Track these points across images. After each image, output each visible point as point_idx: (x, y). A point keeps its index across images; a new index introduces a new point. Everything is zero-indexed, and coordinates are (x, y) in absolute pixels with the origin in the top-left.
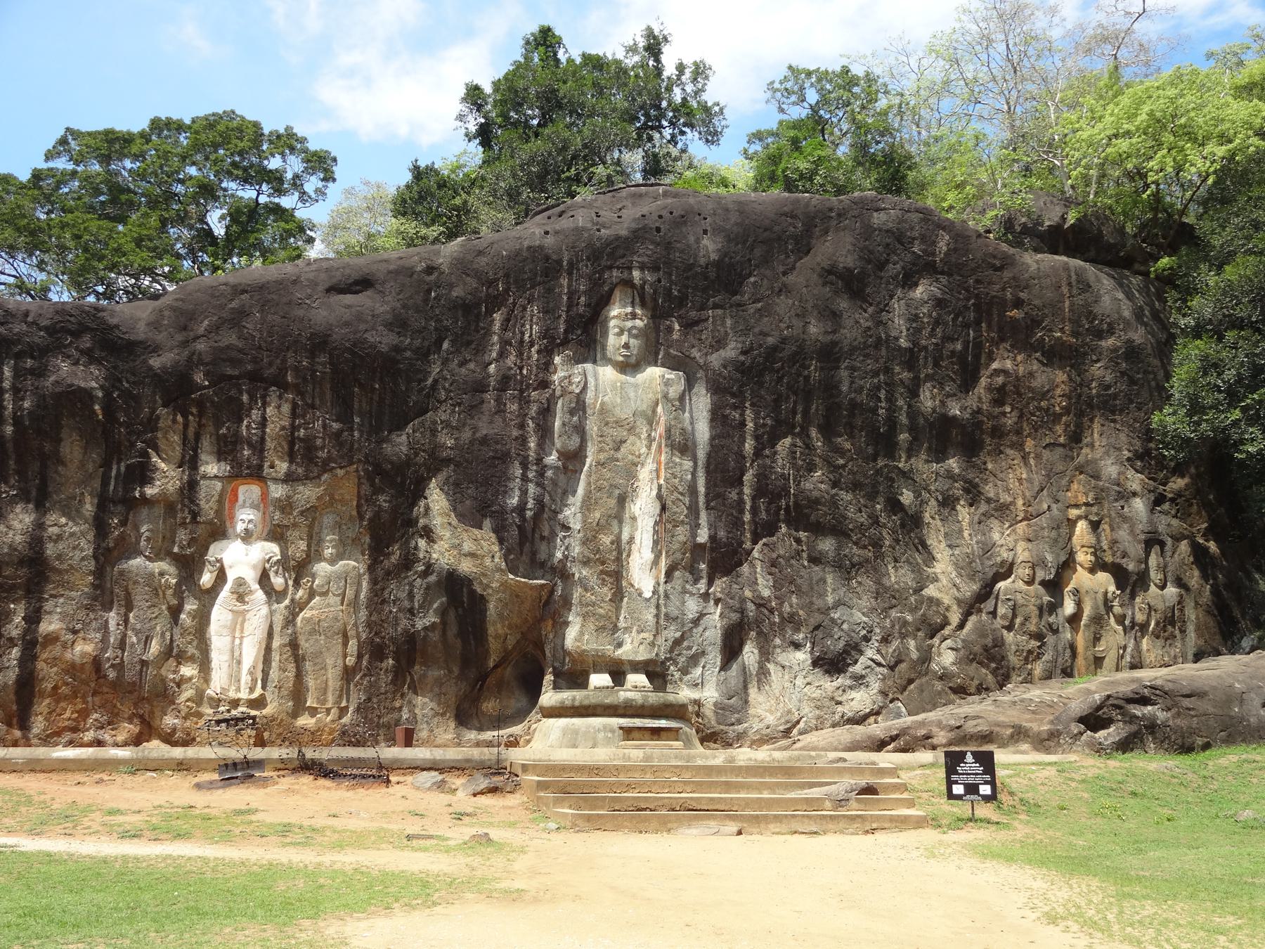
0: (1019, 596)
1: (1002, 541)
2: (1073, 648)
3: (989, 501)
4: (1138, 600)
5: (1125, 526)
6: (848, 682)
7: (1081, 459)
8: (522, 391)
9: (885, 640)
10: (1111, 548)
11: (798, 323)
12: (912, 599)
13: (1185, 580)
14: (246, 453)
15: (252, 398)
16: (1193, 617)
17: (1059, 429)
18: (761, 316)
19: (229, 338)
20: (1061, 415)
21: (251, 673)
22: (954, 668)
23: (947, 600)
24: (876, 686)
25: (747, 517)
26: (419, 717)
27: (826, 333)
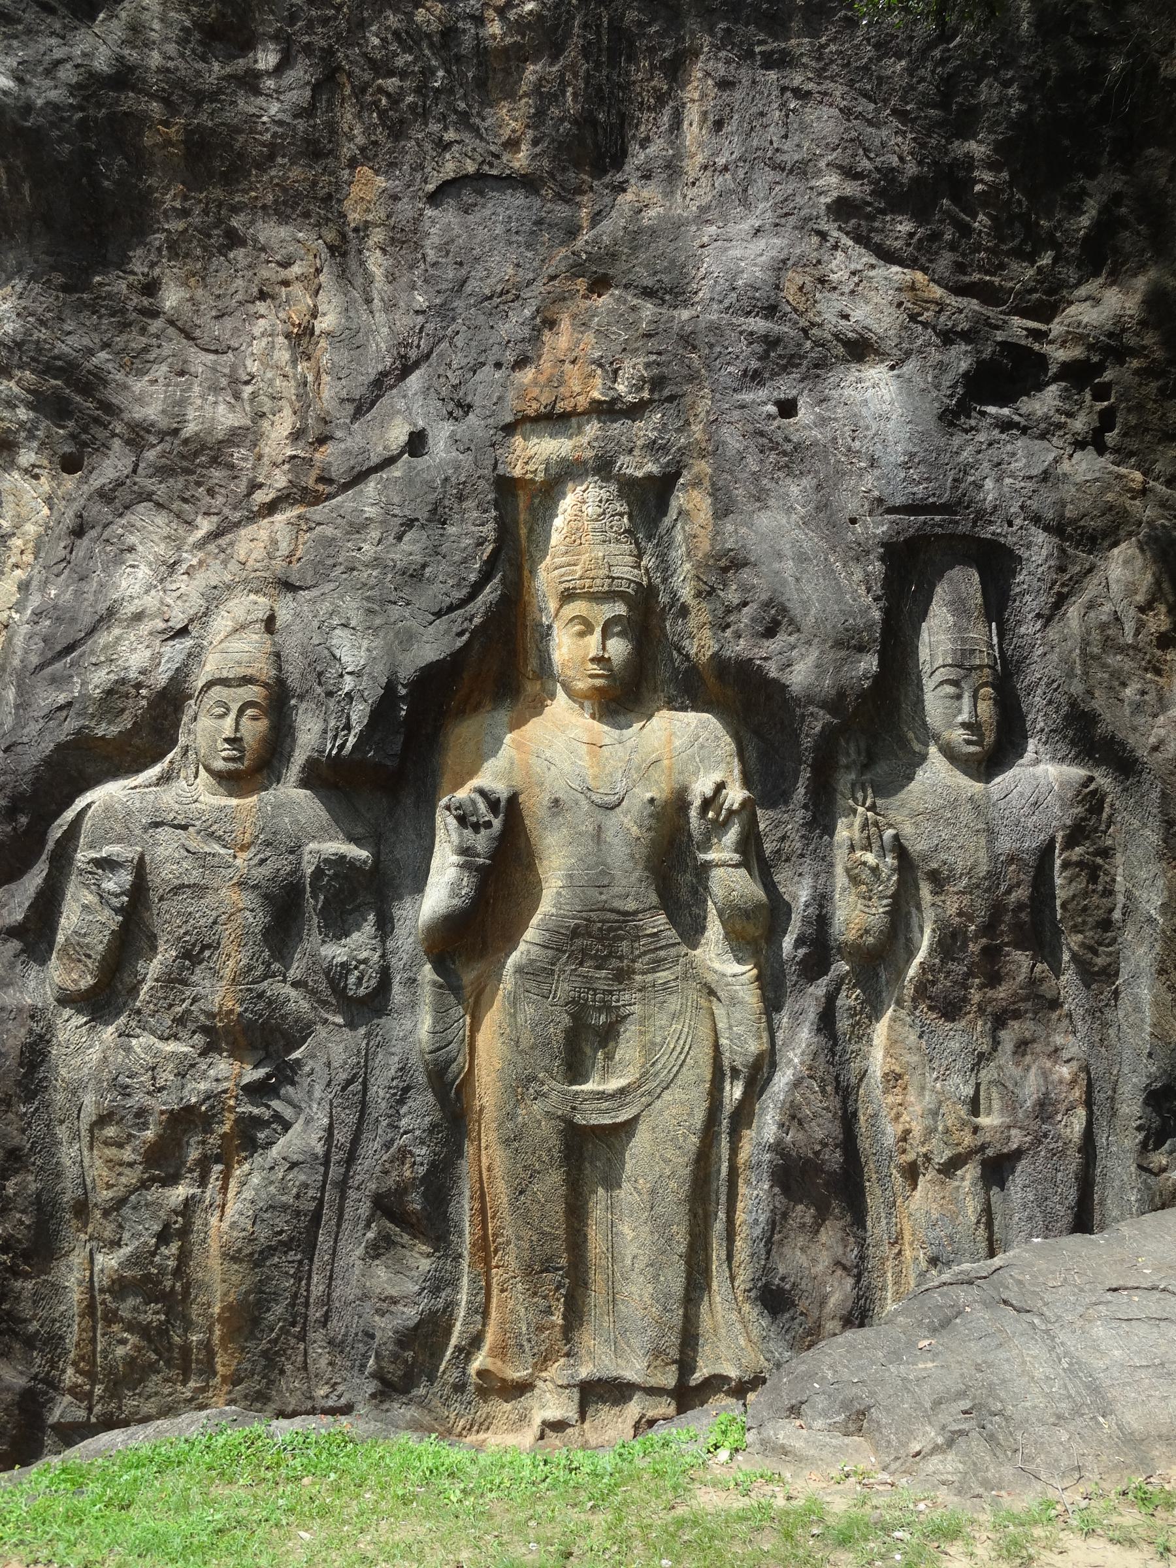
2: (450, 1089)
3: (138, 435)
4: (845, 831)
7: (612, 227)
10: (706, 593)
13: (1114, 719)
16: (1152, 901)
17: (508, 118)
20: (516, 56)
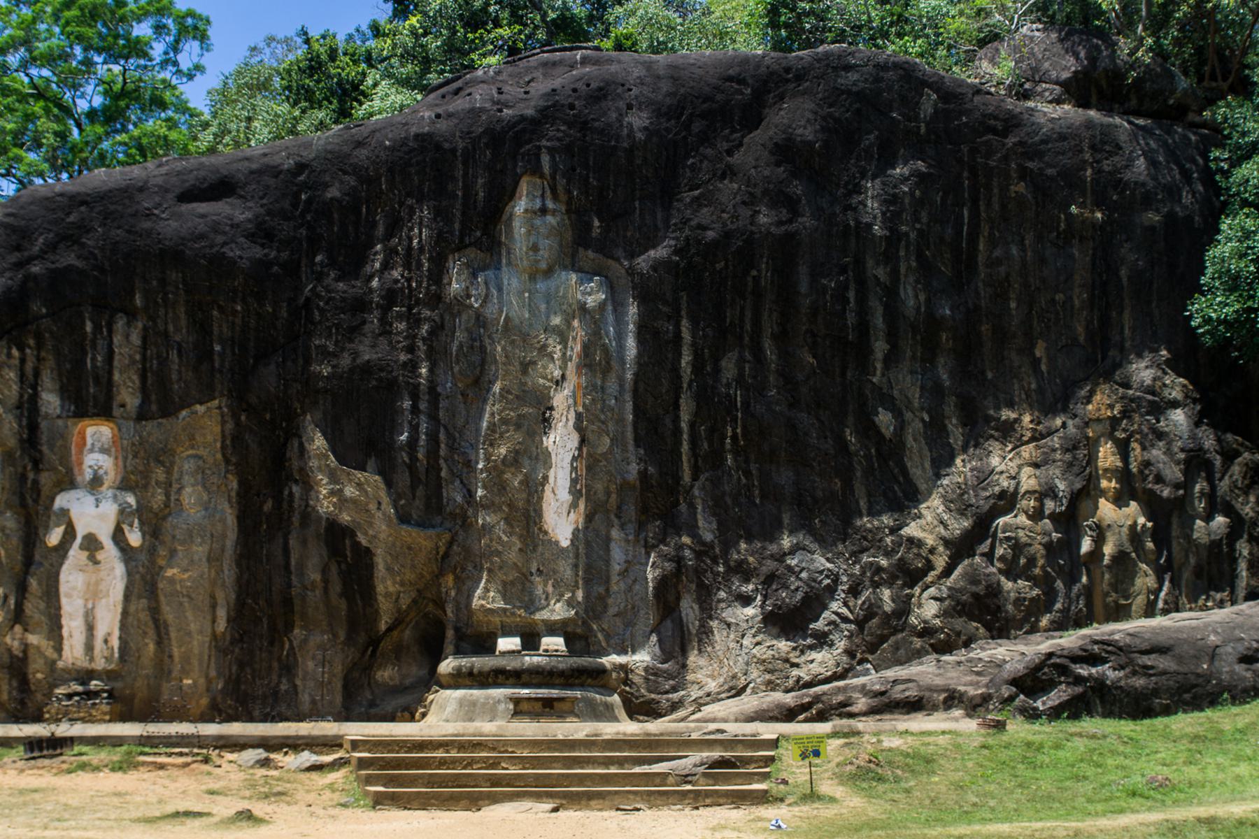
0: (1021, 533)
1: (1002, 467)
5: (1161, 444)
6: (809, 641)
8: (410, 308)
9: (854, 591)
11: (745, 212)
12: (888, 540)
14: (92, 390)
15: (97, 328)
16: (1245, 552)
18: (700, 206)
19: (69, 258)
21: (106, 641)
22: (937, 621)
23: (930, 541)
24: (841, 645)
25: (685, 447)
26: (300, 688)
27: (780, 223)
